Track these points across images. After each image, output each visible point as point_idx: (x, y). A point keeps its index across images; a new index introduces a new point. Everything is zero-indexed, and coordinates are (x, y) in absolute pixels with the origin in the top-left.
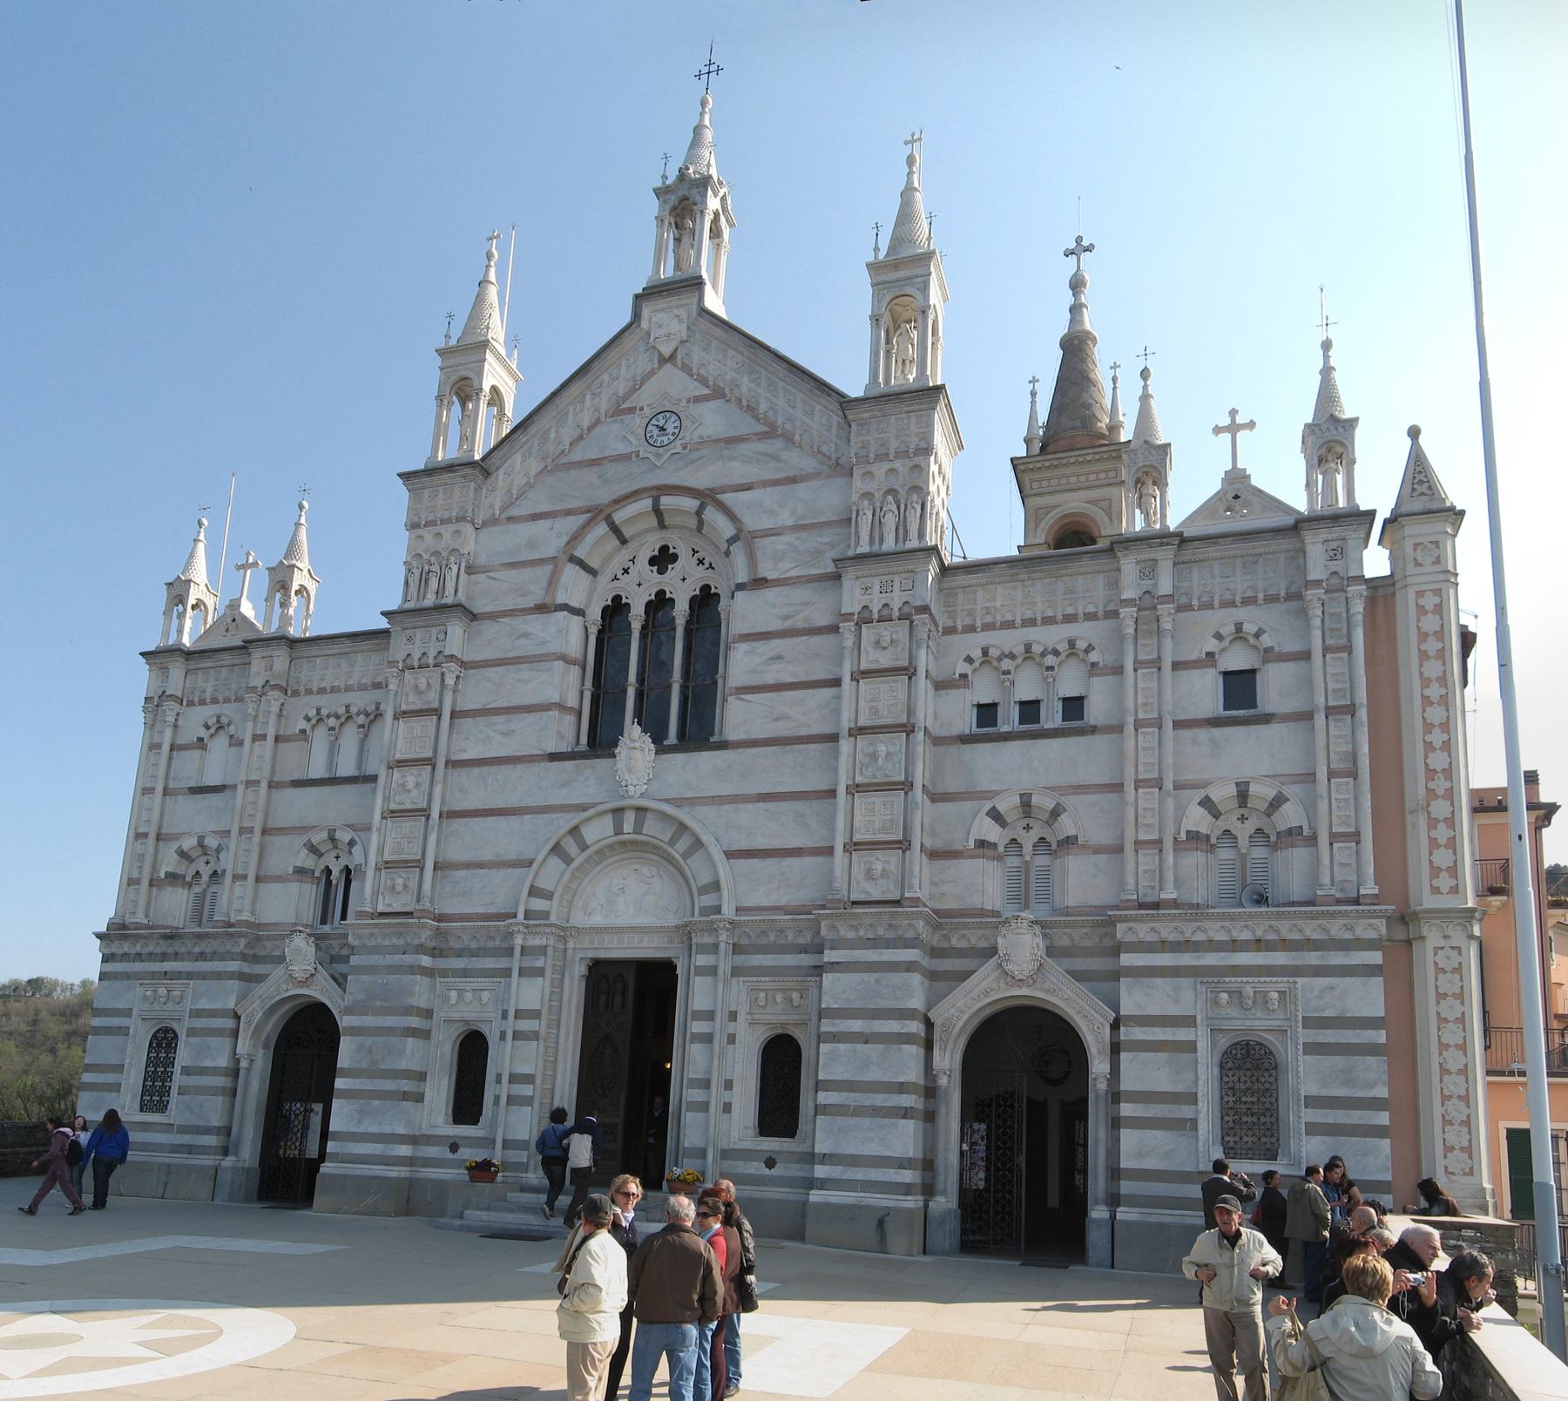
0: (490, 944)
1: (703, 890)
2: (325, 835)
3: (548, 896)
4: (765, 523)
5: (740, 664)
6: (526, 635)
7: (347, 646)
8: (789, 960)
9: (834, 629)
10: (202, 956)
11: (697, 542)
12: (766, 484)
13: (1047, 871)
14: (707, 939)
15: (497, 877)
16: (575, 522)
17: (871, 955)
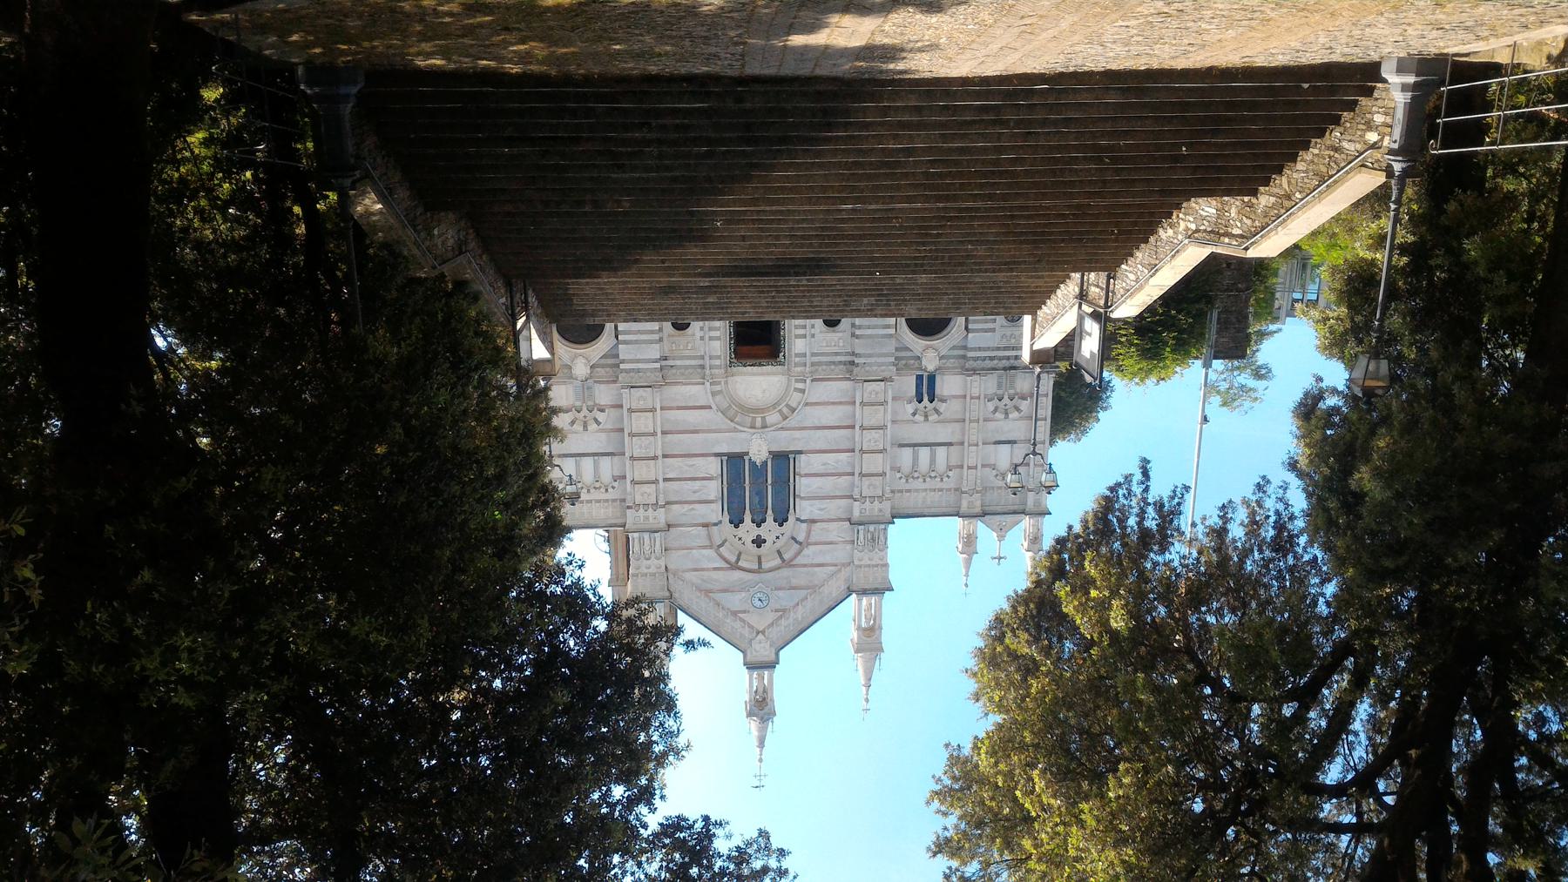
0: (824, 367)
1: (720, 392)
2: (930, 418)
3: (796, 389)
4: (705, 552)
5: (713, 489)
6: (821, 510)
7: (926, 511)
8: (678, 363)
9: (668, 503)
10: (992, 358)
11: (741, 548)
12: (708, 569)
13: (577, 400)
14: (716, 371)
15: (824, 398)
16: (798, 561)
17: (641, 366)
